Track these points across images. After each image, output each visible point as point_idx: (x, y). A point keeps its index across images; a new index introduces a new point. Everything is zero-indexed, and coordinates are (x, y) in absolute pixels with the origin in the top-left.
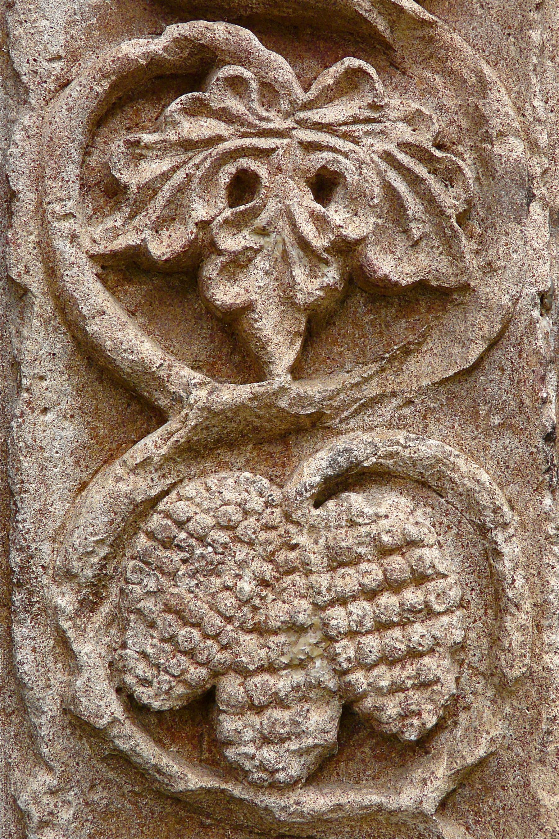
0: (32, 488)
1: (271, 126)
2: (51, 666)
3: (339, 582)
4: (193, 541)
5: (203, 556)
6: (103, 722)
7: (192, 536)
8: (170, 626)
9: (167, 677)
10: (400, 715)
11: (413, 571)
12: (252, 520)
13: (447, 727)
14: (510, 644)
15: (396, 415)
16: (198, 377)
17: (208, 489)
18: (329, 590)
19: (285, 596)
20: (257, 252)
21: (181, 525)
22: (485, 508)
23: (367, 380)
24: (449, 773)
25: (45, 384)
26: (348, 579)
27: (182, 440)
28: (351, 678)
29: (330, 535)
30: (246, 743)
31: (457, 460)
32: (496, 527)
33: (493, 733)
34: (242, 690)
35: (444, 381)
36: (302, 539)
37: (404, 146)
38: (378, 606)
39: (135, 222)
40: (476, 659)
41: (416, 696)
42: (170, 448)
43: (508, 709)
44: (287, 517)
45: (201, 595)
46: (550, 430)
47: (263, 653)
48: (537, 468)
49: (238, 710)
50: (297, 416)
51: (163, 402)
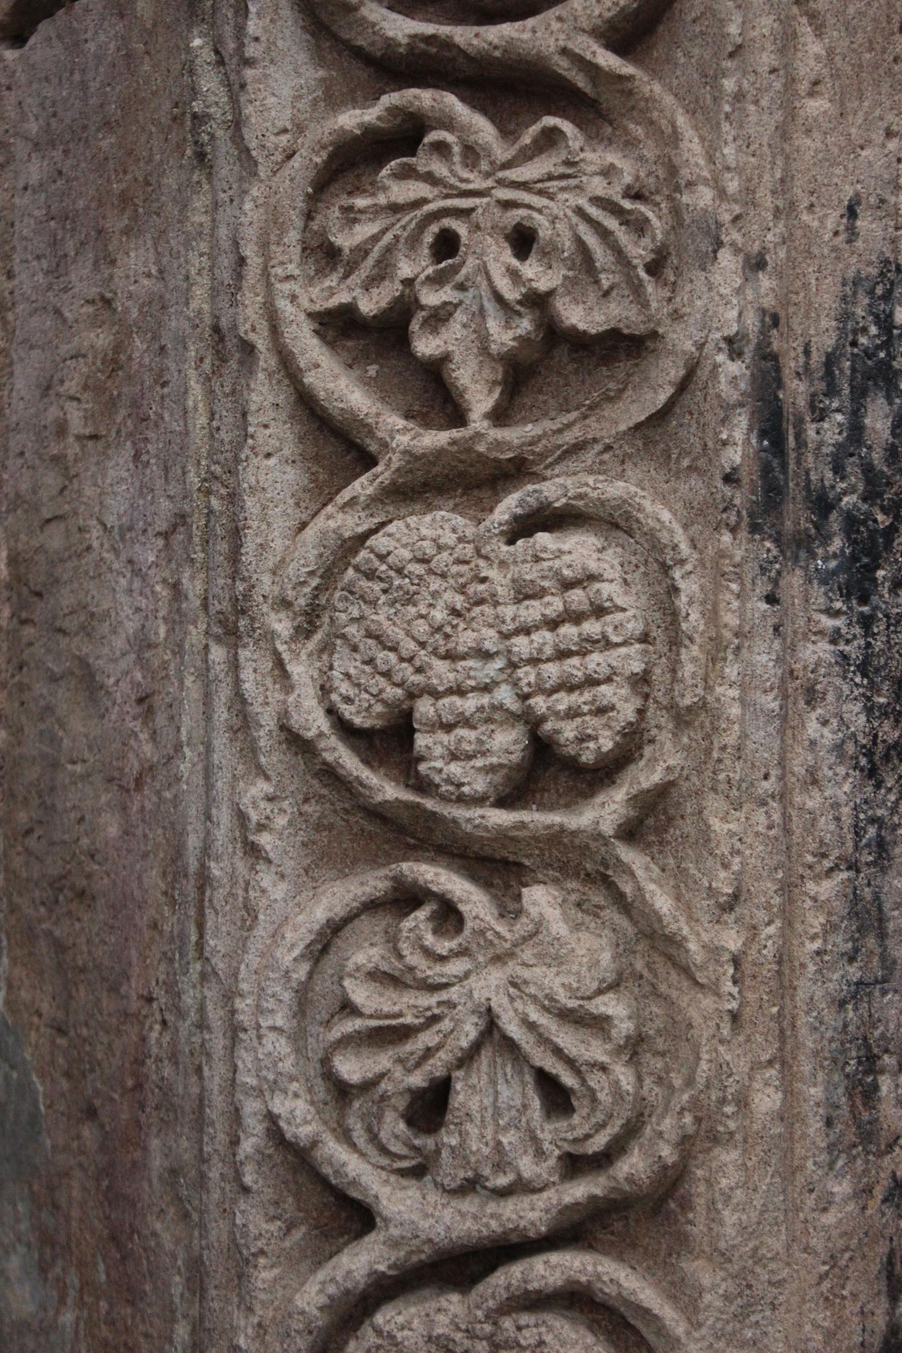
0: (255, 524)
1: (471, 186)
2: (270, 686)
3: (523, 612)
4: (392, 573)
5: (400, 587)
6: (309, 735)
7: (391, 568)
9: (367, 696)
11: (591, 603)
12: (445, 555)
16: (401, 423)
17: (408, 526)
18: (513, 619)
19: (474, 625)
20: (456, 306)
21: (382, 558)
22: (666, 546)
23: (569, 426)
25: (268, 432)
26: (531, 611)
28: (532, 701)
30: (436, 759)
31: (642, 501)
33: (671, 762)
34: (432, 709)
35: (638, 427)
36: (493, 573)
37: (597, 201)
39: (349, 281)
41: (592, 722)
43: (685, 740)
44: (478, 551)
46: (728, 470)
47: (452, 676)
50: (496, 460)
51: (373, 447)
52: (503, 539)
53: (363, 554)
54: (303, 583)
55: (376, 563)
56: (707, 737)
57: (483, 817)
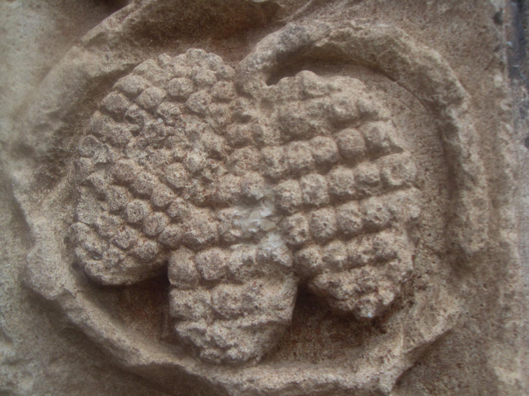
2: (10, 240)
3: (292, 154)
4: (143, 113)
5: (153, 128)
6: (52, 294)
7: (142, 107)
8: (119, 197)
9: (116, 250)
10: (356, 291)
11: (368, 143)
12: (203, 92)
13: (403, 308)
14: (468, 218)
15: (347, 11)
18: (282, 161)
19: (237, 168)
21: (132, 97)
22: (437, 85)
24: (406, 351)
26: (301, 152)
27: (137, 20)
28: (305, 252)
29: (283, 108)
31: (408, 42)
32: (449, 104)
33: (451, 311)
34: (191, 264)
36: (255, 112)
38: (332, 178)
40: (431, 238)
41: (373, 272)
42: (124, 27)
43: (464, 287)
44: (239, 90)
45: (151, 167)
47: (213, 225)
48: (487, 47)
49: (188, 285)
52: (265, 78)
53: (111, 95)
54: (44, 127)
55: (126, 103)
56: (493, 283)
57: (251, 381)
